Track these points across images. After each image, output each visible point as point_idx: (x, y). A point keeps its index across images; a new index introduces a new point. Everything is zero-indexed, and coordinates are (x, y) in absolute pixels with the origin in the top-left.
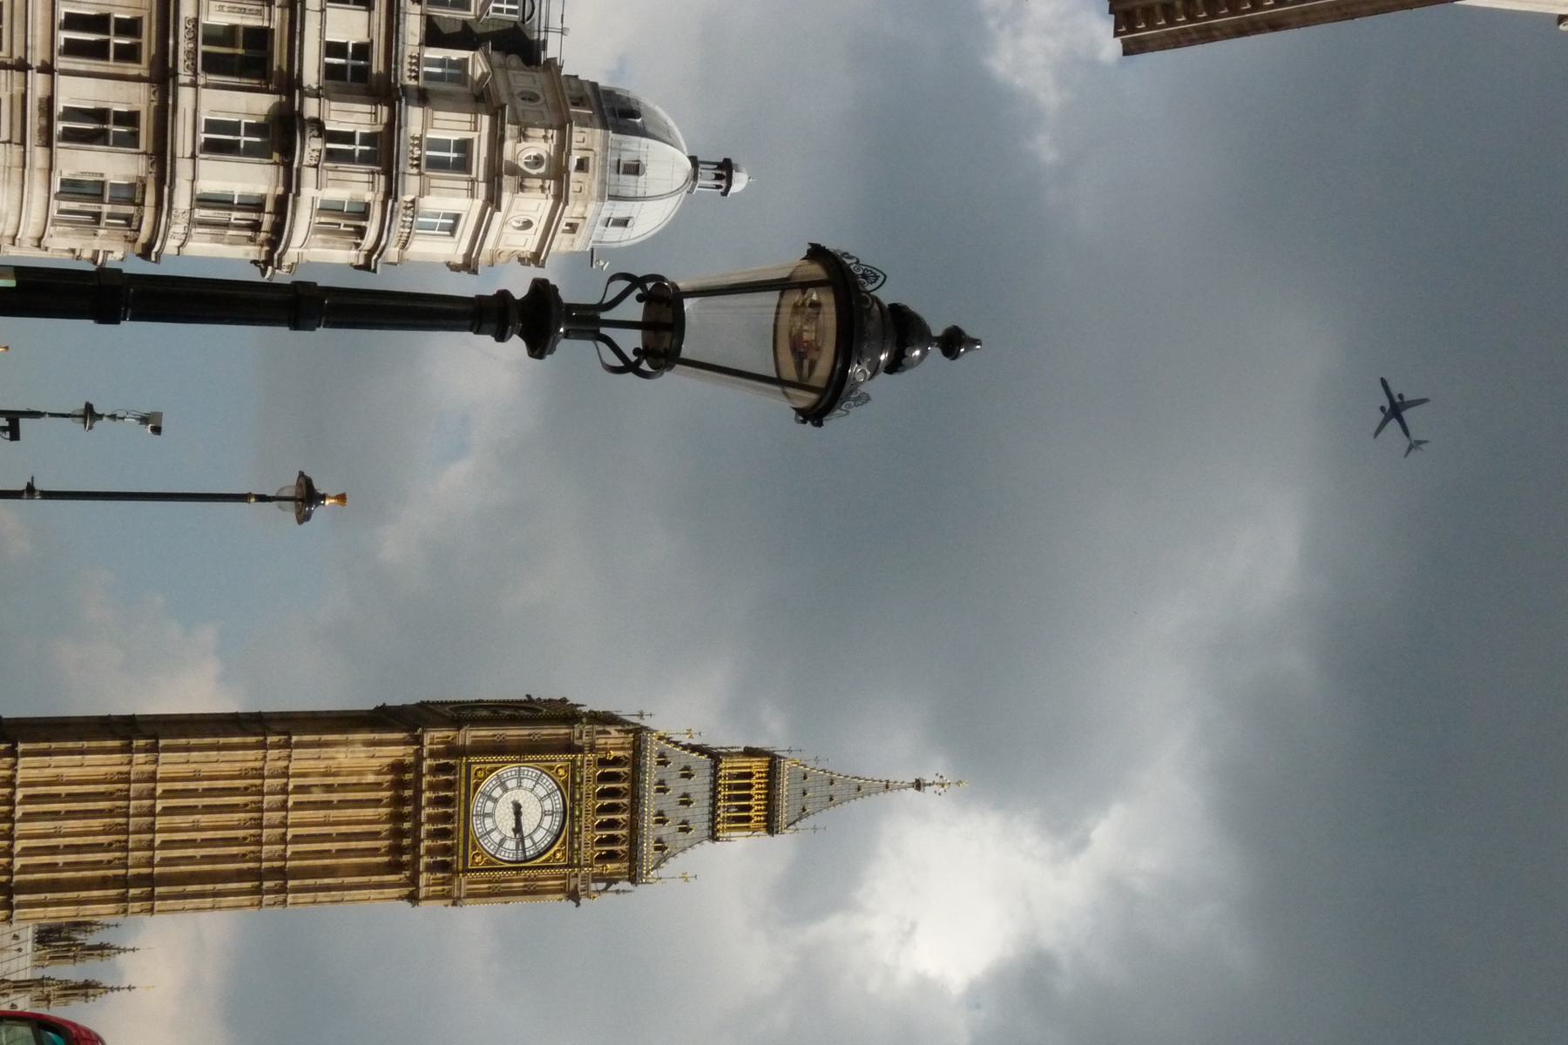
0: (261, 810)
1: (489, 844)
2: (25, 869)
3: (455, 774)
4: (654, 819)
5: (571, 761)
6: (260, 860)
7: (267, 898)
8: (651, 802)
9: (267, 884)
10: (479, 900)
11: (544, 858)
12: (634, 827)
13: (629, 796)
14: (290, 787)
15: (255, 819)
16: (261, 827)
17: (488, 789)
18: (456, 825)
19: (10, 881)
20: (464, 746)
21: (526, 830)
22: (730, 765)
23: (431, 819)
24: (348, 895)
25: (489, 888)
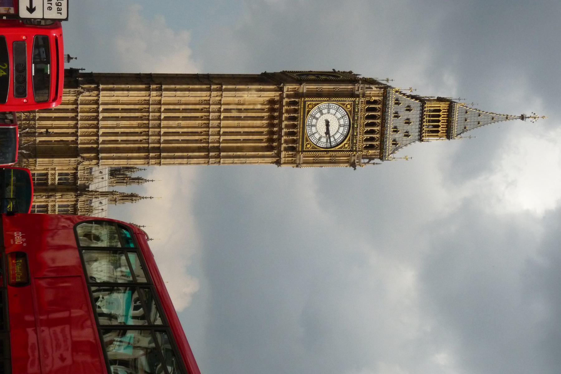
0: (209, 120)
1: (314, 139)
2: (104, 142)
3: (298, 106)
4: (392, 130)
6: (208, 143)
8: (391, 122)
9: (212, 154)
10: (308, 165)
11: (339, 146)
12: (383, 134)
14: (222, 110)
15: (206, 124)
16: (208, 127)
17: (314, 113)
18: (298, 130)
19: (98, 147)
20: (303, 93)
21: (332, 133)
22: (430, 105)
24: (248, 160)
25: (314, 160)
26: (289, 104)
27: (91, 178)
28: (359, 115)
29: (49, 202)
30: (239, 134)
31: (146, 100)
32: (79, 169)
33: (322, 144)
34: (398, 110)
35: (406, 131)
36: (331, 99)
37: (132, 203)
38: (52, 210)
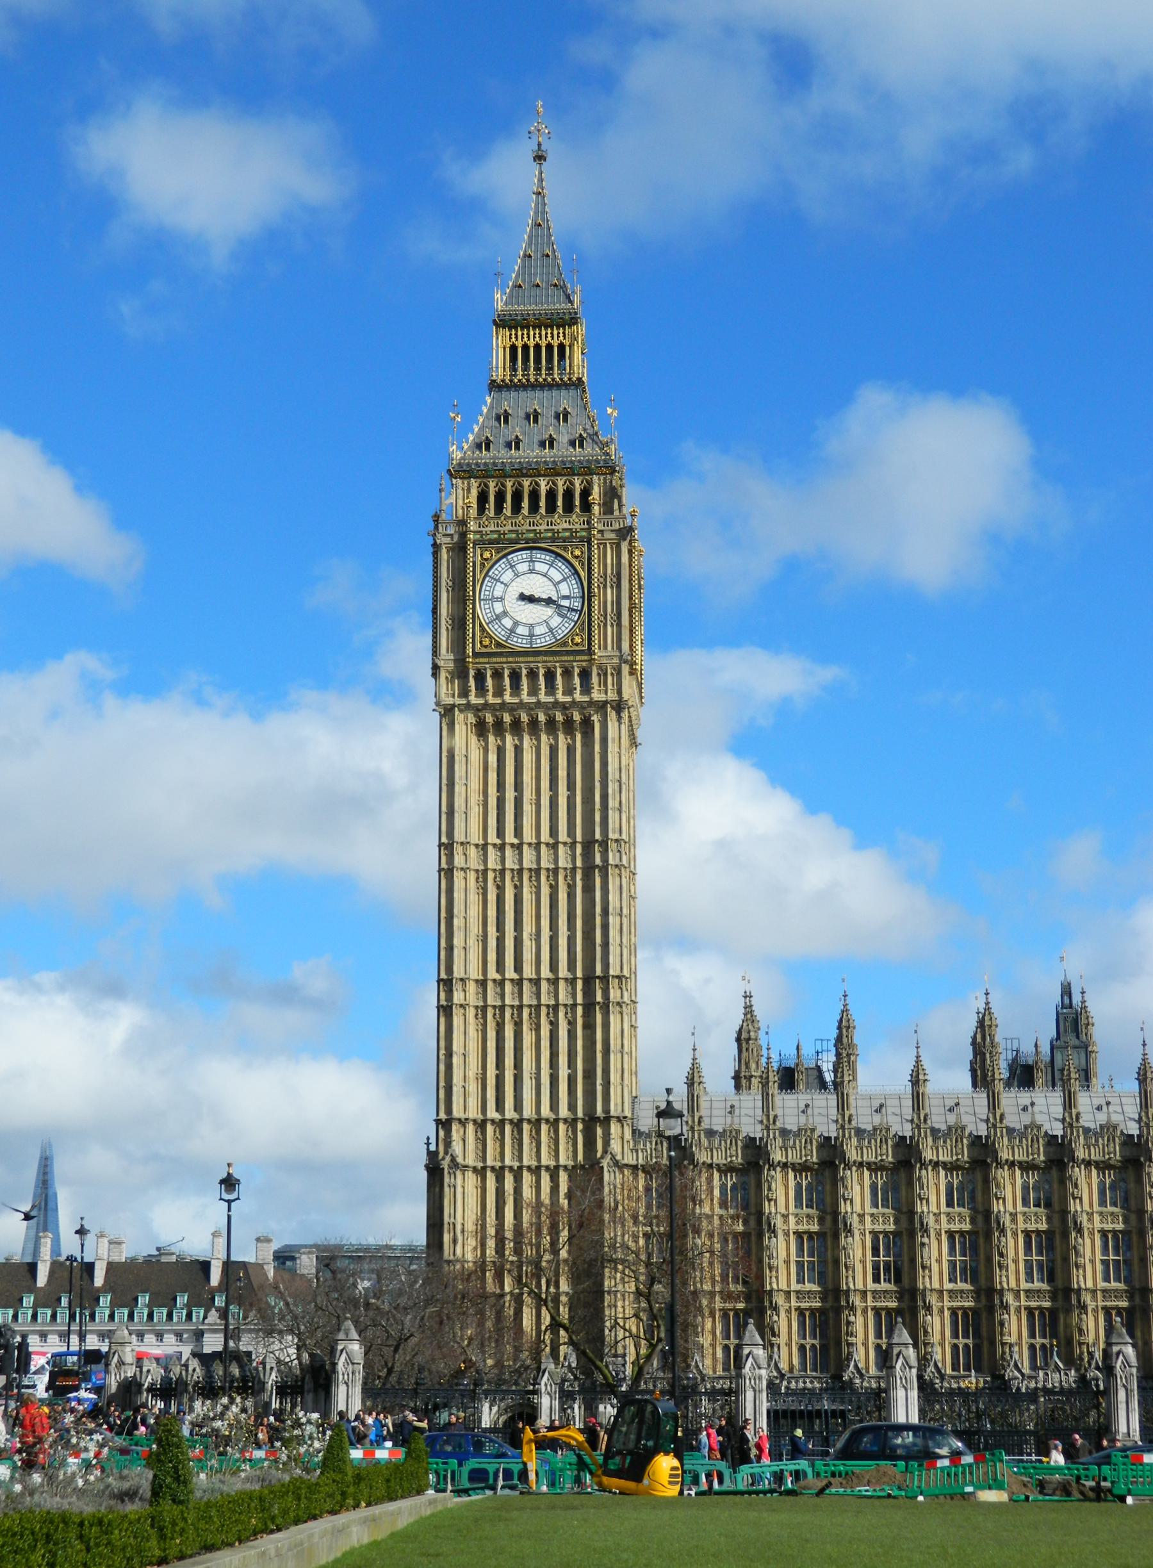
2: (572, 1107)
5: (475, 544)
6: (574, 869)
8: (530, 453)
9: (598, 861)
11: (579, 568)
13: (520, 480)
14: (498, 842)
15: (531, 877)
16: (538, 871)
17: (503, 633)
19: (583, 1120)
20: (455, 661)
22: (500, 370)
23: (534, 691)
25: (612, 625)
26: (481, 689)
28: (560, 527)
29: (788, 1230)
31: (477, 1015)
32: (634, 1162)
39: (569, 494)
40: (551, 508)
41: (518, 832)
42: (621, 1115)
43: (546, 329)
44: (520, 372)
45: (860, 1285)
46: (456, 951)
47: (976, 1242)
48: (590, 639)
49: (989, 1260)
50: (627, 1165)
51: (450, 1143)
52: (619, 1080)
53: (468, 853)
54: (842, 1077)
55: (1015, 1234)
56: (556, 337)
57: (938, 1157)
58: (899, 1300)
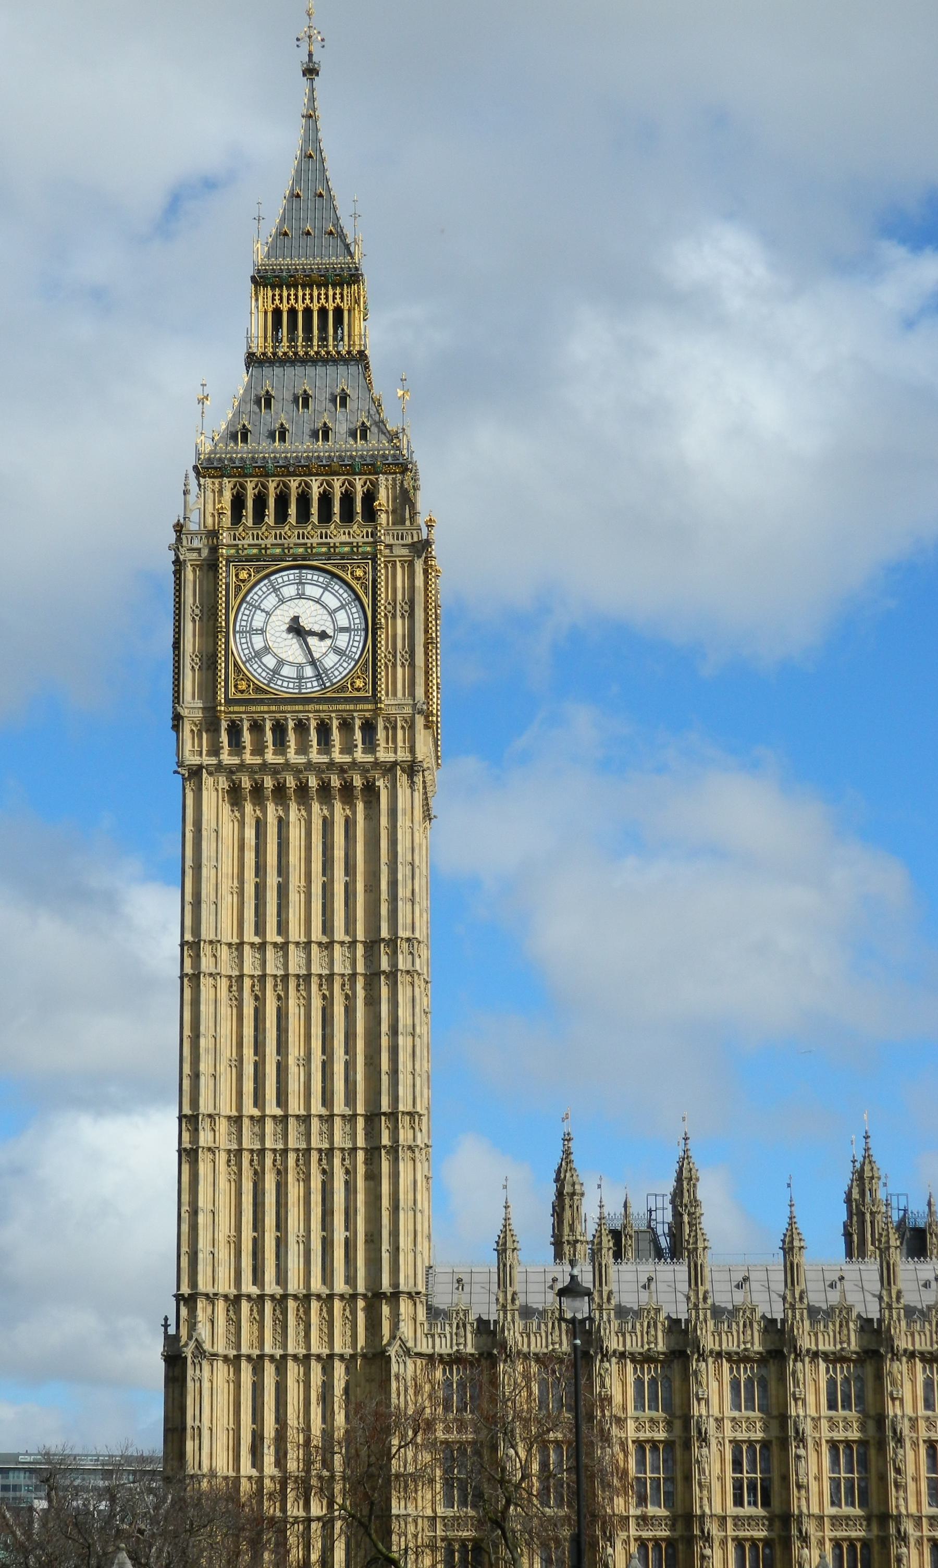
2: (350, 1279)
3: (241, 720)
5: (228, 561)
6: (354, 975)
7: (403, 963)
9: (385, 965)
11: (361, 593)
14: (257, 940)
15: (298, 985)
16: (308, 976)
17: (264, 674)
19: (365, 1296)
20: (204, 709)
22: (261, 340)
23: (303, 749)
25: (403, 665)
26: (236, 744)
27: (744, 1314)
28: (337, 540)
30: (328, 887)
31: (229, 1161)
32: (430, 1351)
33: (356, 644)
34: (264, 430)
35: (330, 401)
36: (221, 627)
37: (582, 1194)
38: (747, 1427)
39: (347, 499)
40: (326, 516)
41: (282, 927)
42: (413, 1290)
43: (319, 287)
44: (285, 343)
45: (718, 1510)
46: (202, 1080)
47: (865, 1454)
48: (374, 683)
49: (883, 1478)
50: (419, 1355)
51: (195, 1324)
52: (411, 1246)
53: (218, 955)
54: (696, 1242)
55: (915, 1444)
56: (331, 299)
57: (817, 1345)
58: (770, 1528)
